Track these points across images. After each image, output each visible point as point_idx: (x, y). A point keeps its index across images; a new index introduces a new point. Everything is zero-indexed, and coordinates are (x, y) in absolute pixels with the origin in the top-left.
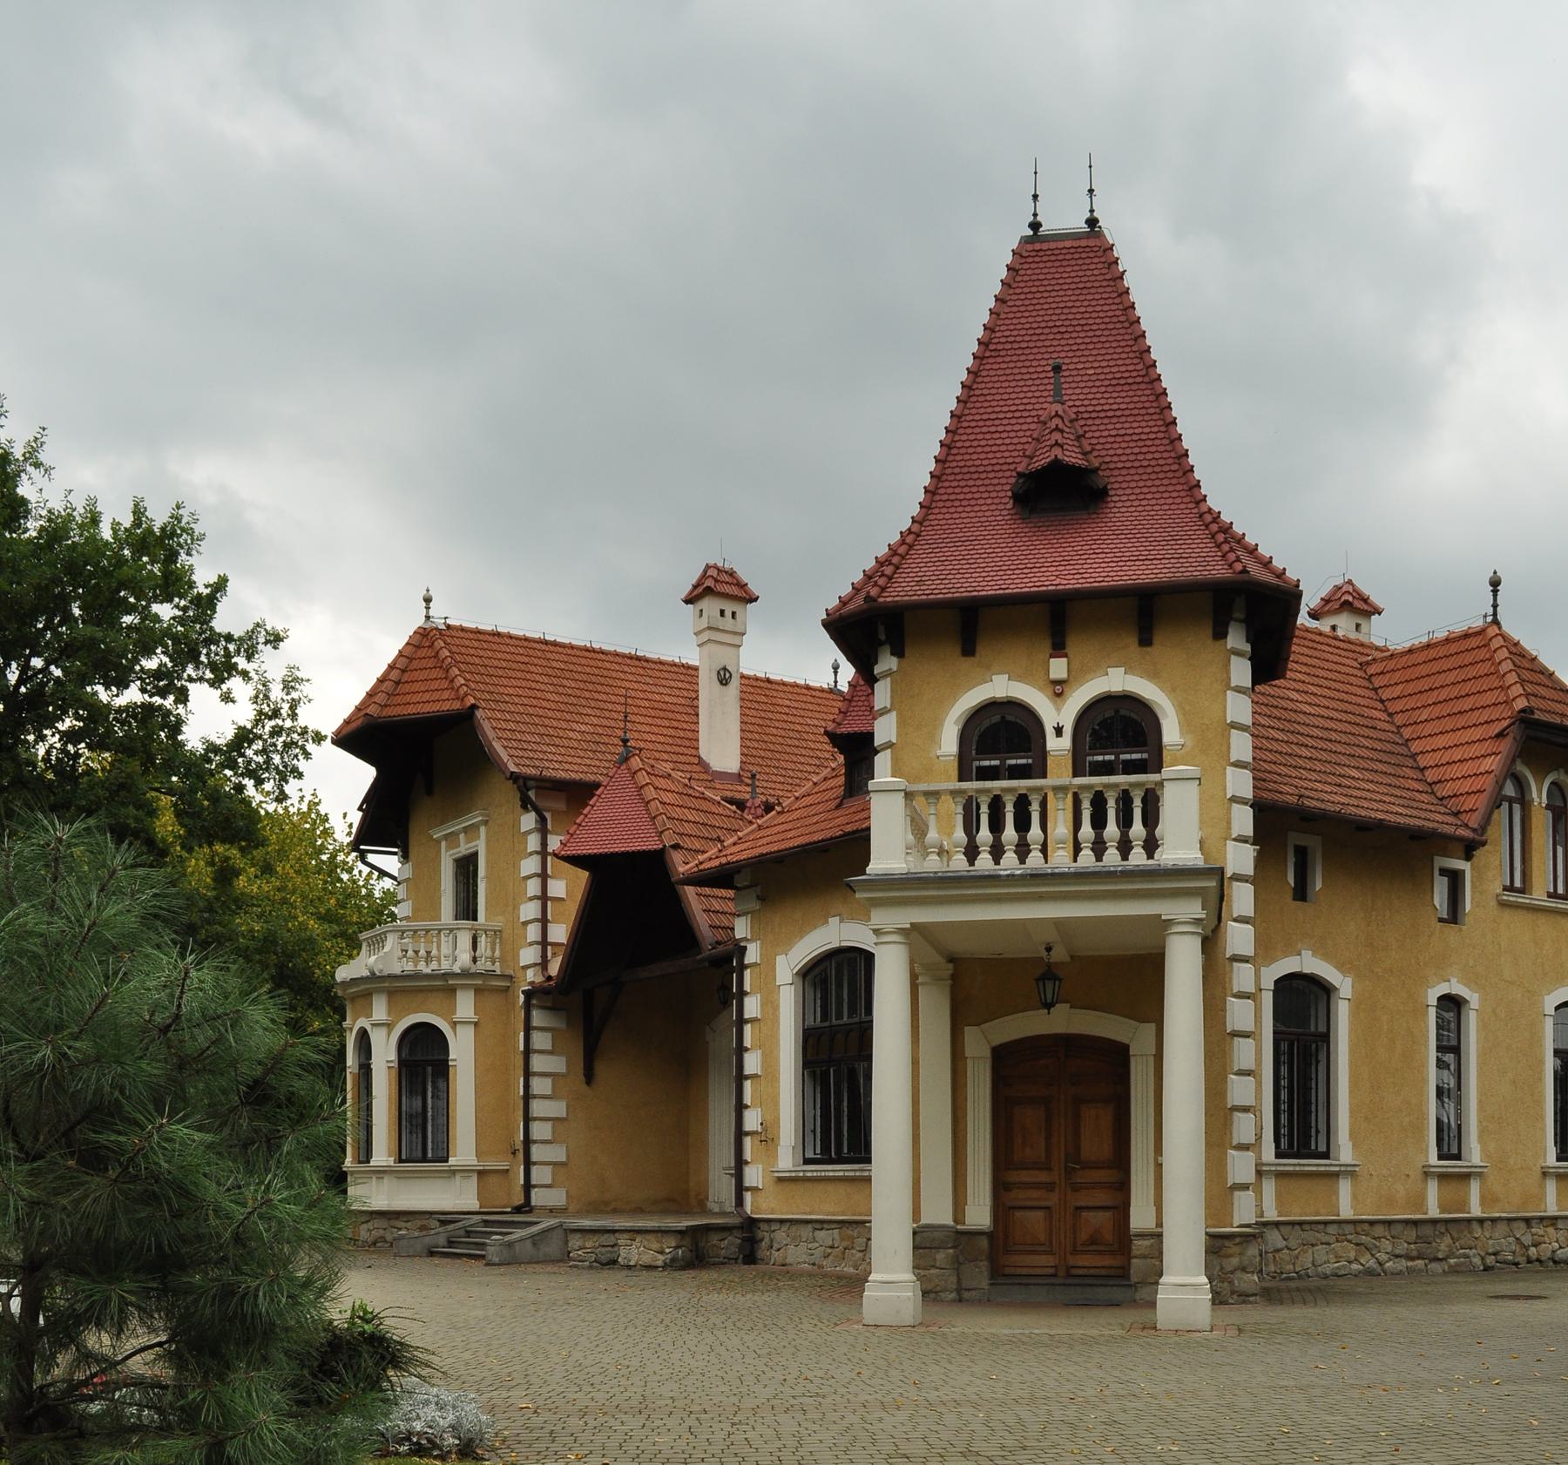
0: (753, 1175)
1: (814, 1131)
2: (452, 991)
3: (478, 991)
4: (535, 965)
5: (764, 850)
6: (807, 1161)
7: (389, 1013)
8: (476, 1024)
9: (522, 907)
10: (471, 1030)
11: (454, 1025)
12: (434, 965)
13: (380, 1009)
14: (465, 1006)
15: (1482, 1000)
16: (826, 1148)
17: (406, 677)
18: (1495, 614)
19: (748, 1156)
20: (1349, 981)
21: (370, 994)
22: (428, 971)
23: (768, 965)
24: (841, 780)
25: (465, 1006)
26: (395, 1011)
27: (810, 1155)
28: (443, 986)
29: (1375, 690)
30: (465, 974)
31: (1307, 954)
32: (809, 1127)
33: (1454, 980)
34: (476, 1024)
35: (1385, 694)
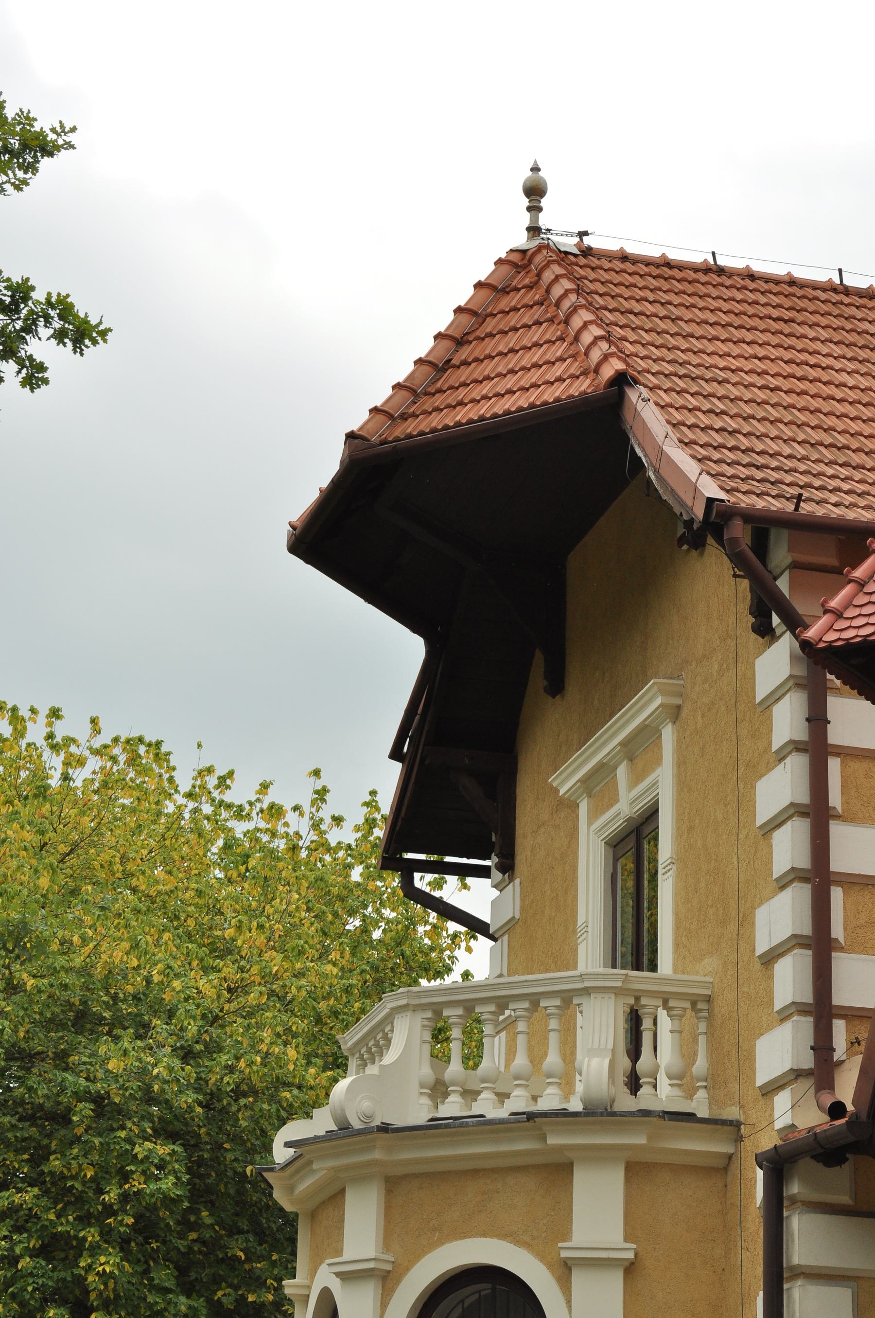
2: (558, 1172)
3: (638, 1170)
4: (797, 1074)
7: (388, 1237)
8: (630, 1269)
9: (761, 915)
10: (615, 1282)
11: (564, 1270)
12: (519, 1102)
13: (361, 1231)
14: (598, 1210)
17: (465, 353)
21: (342, 1191)
22: (502, 1113)
25: (598, 1210)
26: (405, 1233)
28: (532, 1161)
30: (597, 1113)
34: (630, 1269)
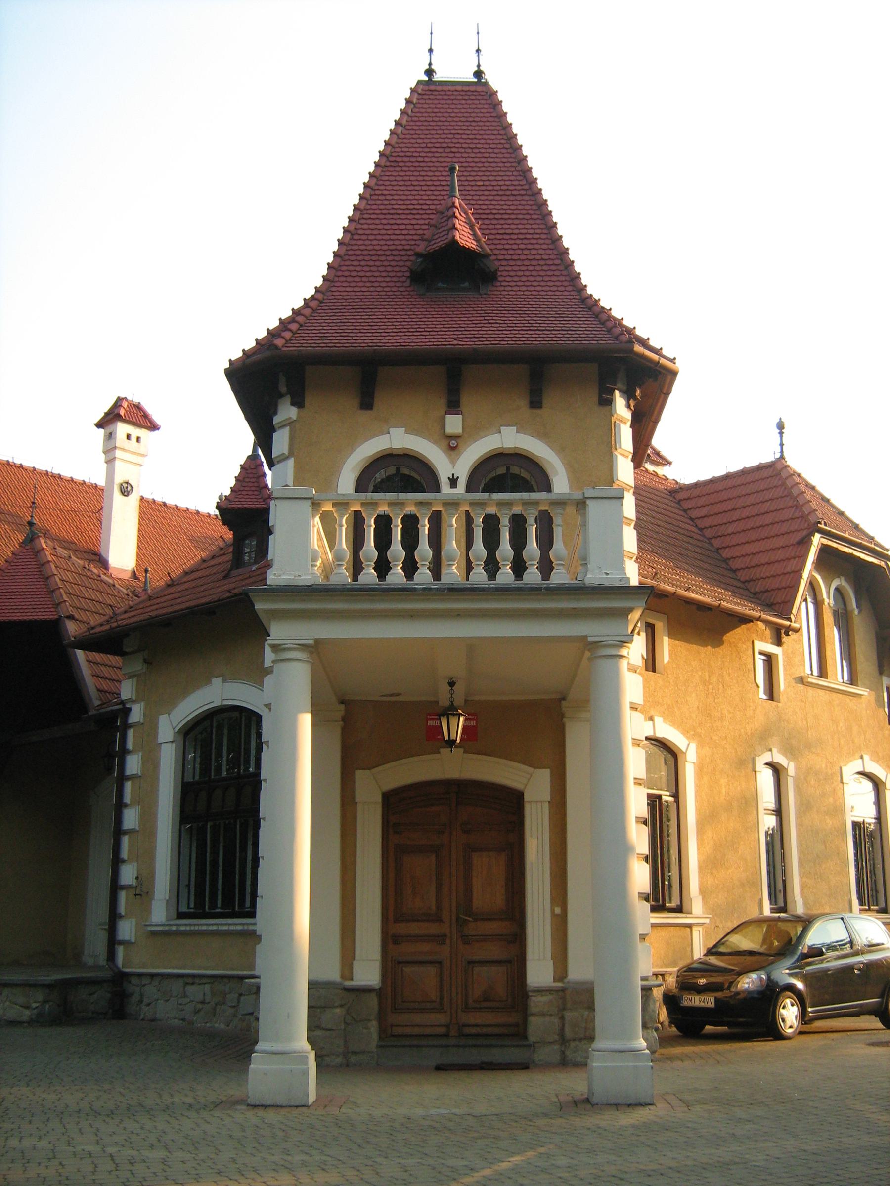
0: (126, 930)
1: (189, 886)
5: (153, 614)
6: (180, 915)
15: (797, 769)
16: (200, 903)
18: (782, 452)
19: (122, 909)
20: (693, 747)
23: (150, 726)
24: (229, 557)
27: (183, 909)
29: (685, 511)
31: (658, 720)
32: (184, 881)
33: (775, 750)
35: (694, 514)
